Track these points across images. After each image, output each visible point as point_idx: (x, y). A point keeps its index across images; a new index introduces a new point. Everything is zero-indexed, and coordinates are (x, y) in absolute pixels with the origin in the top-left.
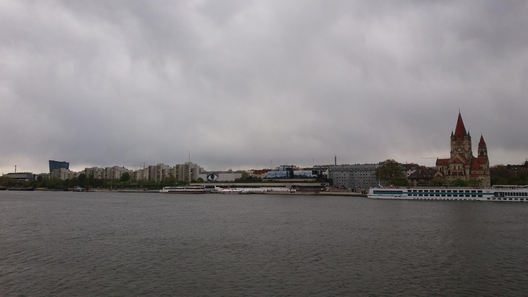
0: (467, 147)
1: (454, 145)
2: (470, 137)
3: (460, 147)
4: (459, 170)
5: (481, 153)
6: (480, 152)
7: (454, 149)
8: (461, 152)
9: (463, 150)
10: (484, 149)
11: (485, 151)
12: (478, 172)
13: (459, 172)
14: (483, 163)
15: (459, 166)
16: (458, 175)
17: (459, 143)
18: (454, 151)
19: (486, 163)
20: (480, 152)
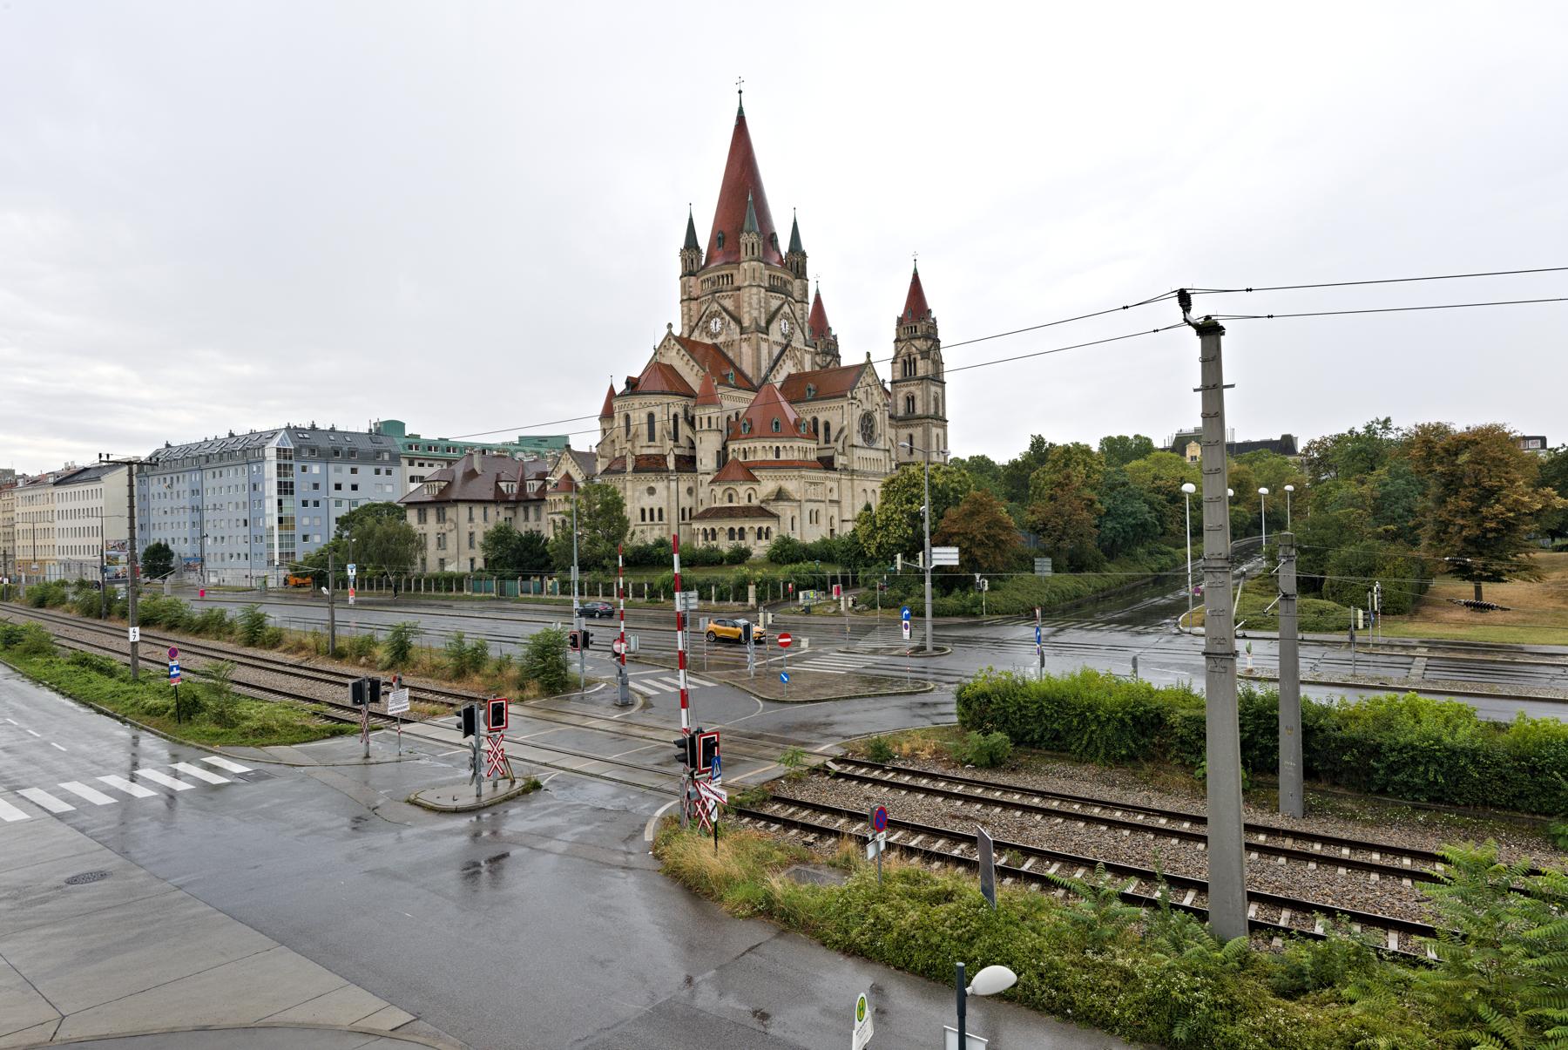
0: (750, 304)
1: (690, 299)
2: (804, 255)
3: (715, 307)
4: (652, 437)
6: (899, 360)
7: (693, 324)
8: (721, 339)
9: (733, 324)
10: (917, 343)
11: (921, 352)
13: (652, 451)
14: (835, 397)
15: (651, 416)
16: (630, 468)
17: (713, 283)
18: (691, 332)
20: (899, 360)
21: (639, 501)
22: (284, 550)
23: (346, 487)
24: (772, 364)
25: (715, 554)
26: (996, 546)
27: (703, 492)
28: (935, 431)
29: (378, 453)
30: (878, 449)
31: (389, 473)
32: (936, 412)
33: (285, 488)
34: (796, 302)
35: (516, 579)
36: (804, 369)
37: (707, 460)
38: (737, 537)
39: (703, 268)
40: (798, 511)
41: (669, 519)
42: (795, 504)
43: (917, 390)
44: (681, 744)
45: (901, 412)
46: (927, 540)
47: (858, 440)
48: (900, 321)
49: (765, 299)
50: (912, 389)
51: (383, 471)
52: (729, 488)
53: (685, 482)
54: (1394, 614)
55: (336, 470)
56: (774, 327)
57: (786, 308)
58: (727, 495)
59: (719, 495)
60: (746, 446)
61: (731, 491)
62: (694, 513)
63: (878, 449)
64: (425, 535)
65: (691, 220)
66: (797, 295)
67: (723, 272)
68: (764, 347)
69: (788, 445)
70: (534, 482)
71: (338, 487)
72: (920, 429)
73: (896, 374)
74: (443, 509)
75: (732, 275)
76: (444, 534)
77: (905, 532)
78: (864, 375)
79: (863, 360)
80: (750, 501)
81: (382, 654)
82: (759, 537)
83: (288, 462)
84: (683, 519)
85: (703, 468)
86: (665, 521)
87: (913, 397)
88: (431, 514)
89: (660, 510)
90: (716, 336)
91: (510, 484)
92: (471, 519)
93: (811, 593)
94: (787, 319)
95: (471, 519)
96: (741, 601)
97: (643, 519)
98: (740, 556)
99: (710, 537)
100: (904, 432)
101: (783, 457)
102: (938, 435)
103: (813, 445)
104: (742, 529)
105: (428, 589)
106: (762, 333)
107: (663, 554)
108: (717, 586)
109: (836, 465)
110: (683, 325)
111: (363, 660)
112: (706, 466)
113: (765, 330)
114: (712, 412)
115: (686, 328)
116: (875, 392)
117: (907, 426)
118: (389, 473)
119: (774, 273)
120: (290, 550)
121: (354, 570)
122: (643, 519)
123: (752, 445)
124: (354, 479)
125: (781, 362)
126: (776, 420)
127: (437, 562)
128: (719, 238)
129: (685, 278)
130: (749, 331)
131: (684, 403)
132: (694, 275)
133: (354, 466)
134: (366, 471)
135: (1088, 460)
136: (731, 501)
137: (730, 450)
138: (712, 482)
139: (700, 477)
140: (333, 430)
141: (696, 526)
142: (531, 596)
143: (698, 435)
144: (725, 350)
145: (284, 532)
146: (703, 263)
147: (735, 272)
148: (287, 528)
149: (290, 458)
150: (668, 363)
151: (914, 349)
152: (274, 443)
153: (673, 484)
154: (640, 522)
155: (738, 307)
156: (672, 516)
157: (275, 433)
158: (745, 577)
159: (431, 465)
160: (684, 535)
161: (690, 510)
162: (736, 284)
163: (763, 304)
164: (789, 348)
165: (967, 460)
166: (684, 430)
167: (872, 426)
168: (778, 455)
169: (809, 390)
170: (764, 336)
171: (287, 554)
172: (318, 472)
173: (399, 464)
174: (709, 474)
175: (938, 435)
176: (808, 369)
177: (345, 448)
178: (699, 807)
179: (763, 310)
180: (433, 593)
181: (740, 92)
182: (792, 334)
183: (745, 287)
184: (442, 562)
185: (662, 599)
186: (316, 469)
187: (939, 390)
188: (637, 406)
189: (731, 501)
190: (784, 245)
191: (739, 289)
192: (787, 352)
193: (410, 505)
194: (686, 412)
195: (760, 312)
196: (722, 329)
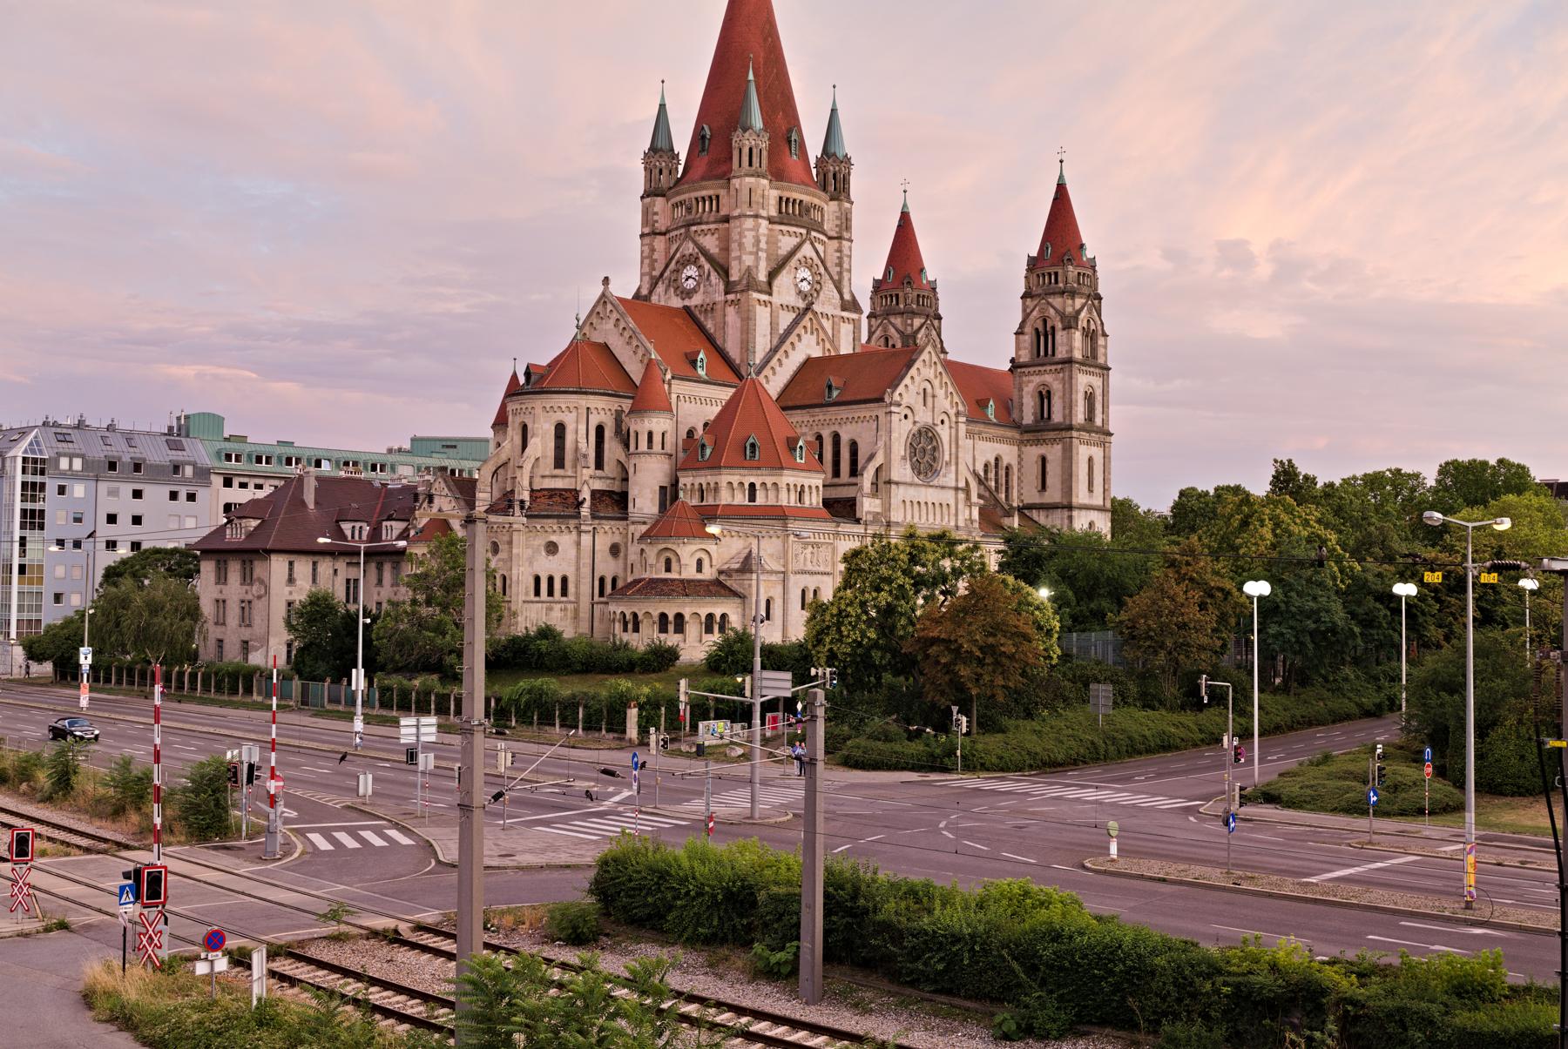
0: (741, 245)
1: (654, 233)
2: (847, 161)
3: (689, 248)
4: (559, 462)
5: (1037, 329)
6: (1028, 329)
7: (656, 273)
8: (696, 300)
9: (714, 277)
10: (1057, 301)
11: (1062, 315)
12: (730, 487)
13: (559, 484)
15: (560, 429)
17: (689, 210)
19: (881, 400)
20: (1028, 329)
21: (531, 563)
22: (25, 616)
23: (124, 520)
24: (775, 342)
25: (621, 654)
26: (997, 663)
27: (633, 551)
28: (1083, 452)
29: (176, 468)
30: (943, 488)
31: (191, 497)
32: (1090, 417)
33: (33, 519)
34: (830, 238)
35: (324, 680)
36: (837, 349)
37: (645, 502)
38: (671, 628)
39: (679, 180)
40: (779, 589)
41: (577, 594)
42: (773, 578)
43: (1054, 382)
44: (126, 875)
45: (1028, 418)
46: (758, 660)
47: (901, 470)
48: (1033, 264)
49: (769, 236)
50: (1048, 378)
51: (183, 496)
52: (666, 549)
53: (608, 534)
54: (1512, 795)
55: (113, 493)
56: (784, 280)
57: (807, 250)
58: (663, 560)
59: (652, 559)
60: (703, 481)
61: (668, 554)
62: (620, 584)
63: (943, 488)
64: (224, 601)
65: (662, 107)
66: (829, 226)
67: (704, 193)
68: (762, 316)
69: (769, 481)
70: (393, 523)
71: (112, 519)
72: (1058, 448)
73: (1022, 352)
74: (251, 562)
75: (718, 197)
76: (250, 602)
77: (863, 635)
78: (918, 364)
80: (699, 569)
81: (43, 778)
82: (709, 630)
83: (38, 479)
84: (601, 594)
85: (636, 511)
86: (571, 597)
87: (1049, 392)
88: (234, 570)
89: (564, 580)
90: (688, 294)
91: (358, 525)
92: (291, 580)
93: (721, 726)
94: (810, 268)
95: (291, 580)
96: (615, 731)
97: (537, 593)
98: (662, 659)
99: (630, 626)
100: (1033, 452)
101: (757, 503)
102: (1090, 460)
103: (817, 480)
104: (679, 617)
105: (206, 688)
106: (760, 292)
107: (543, 648)
108: (585, 707)
109: (858, 515)
110: (642, 275)
111: (24, 786)
112: (641, 509)
113: (765, 287)
114: (658, 423)
115: (647, 278)
116: (940, 393)
117: (1037, 442)
118: (191, 497)
119: (786, 194)
120: (34, 616)
121: (90, 656)
122: (537, 593)
123: (711, 479)
124: (138, 507)
125: (793, 338)
126: (751, 440)
127: (238, 646)
128: (699, 140)
129: (648, 200)
130: (739, 288)
131: (616, 407)
132: (664, 196)
133: (138, 487)
134: (156, 493)
135: (1285, 517)
136: (668, 569)
137: (680, 485)
138: (643, 537)
139: (632, 528)
140: (111, 428)
141: (612, 608)
142: (341, 708)
143: (633, 461)
144: (702, 319)
145: (26, 588)
146: (679, 176)
147: (722, 192)
148: (31, 582)
149: (42, 473)
150: (601, 341)
151: (1052, 311)
152: (19, 451)
153: (586, 539)
154: (532, 597)
155: (726, 249)
156: (583, 589)
157: (23, 432)
158: (622, 695)
159: (259, 487)
160: (601, 620)
161: (614, 580)
162: (723, 212)
163: (763, 245)
164: (809, 315)
165: (1212, 492)
166: (612, 449)
167: (934, 449)
168: (752, 498)
169: (830, 387)
170: (764, 297)
171: (30, 621)
172: (82, 495)
173: (208, 484)
174: (644, 523)
175: (1090, 460)
176: (846, 348)
177: (126, 459)
178: (145, 942)
179: (763, 255)
180: (212, 695)
182: (818, 293)
183: (735, 218)
184: (246, 646)
185: (513, 724)
186: (78, 490)
187: (1097, 382)
188: (538, 411)
189: (668, 569)
190: (814, 150)
191: (727, 219)
192: (806, 321)
193: (207, 553)
194: (618, 422)
195: (757, 259)
196: (698, 284)
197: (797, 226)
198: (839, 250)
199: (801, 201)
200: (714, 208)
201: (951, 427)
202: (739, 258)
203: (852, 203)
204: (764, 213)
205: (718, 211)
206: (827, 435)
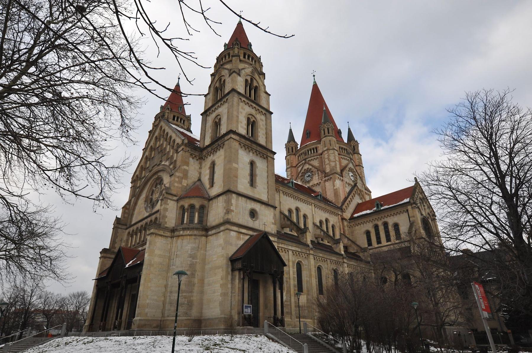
1: (292, 167)
34: (356, 166)
75: (316, 148)
79: (413, 184)
94: (353, 172)
119: (342, 146)
132: (294, 154)
147: (318, 145)
164: (356, 188)
181: (314, 76)
191: (321, 154)
192: (355, 189)
197: (347, 157)
198: (360, 169)
199: (346, 150)
200: (315, 151)
201: (432, 221)
202: (329, 164)
203: (361, 155)
204: (336, 149)
205: (317, 152)
206: (380, 223)
